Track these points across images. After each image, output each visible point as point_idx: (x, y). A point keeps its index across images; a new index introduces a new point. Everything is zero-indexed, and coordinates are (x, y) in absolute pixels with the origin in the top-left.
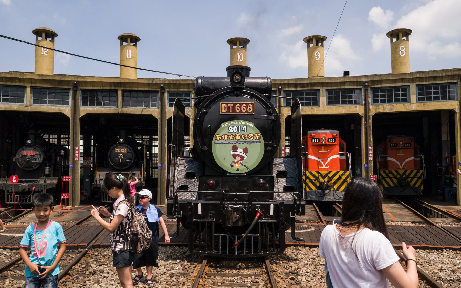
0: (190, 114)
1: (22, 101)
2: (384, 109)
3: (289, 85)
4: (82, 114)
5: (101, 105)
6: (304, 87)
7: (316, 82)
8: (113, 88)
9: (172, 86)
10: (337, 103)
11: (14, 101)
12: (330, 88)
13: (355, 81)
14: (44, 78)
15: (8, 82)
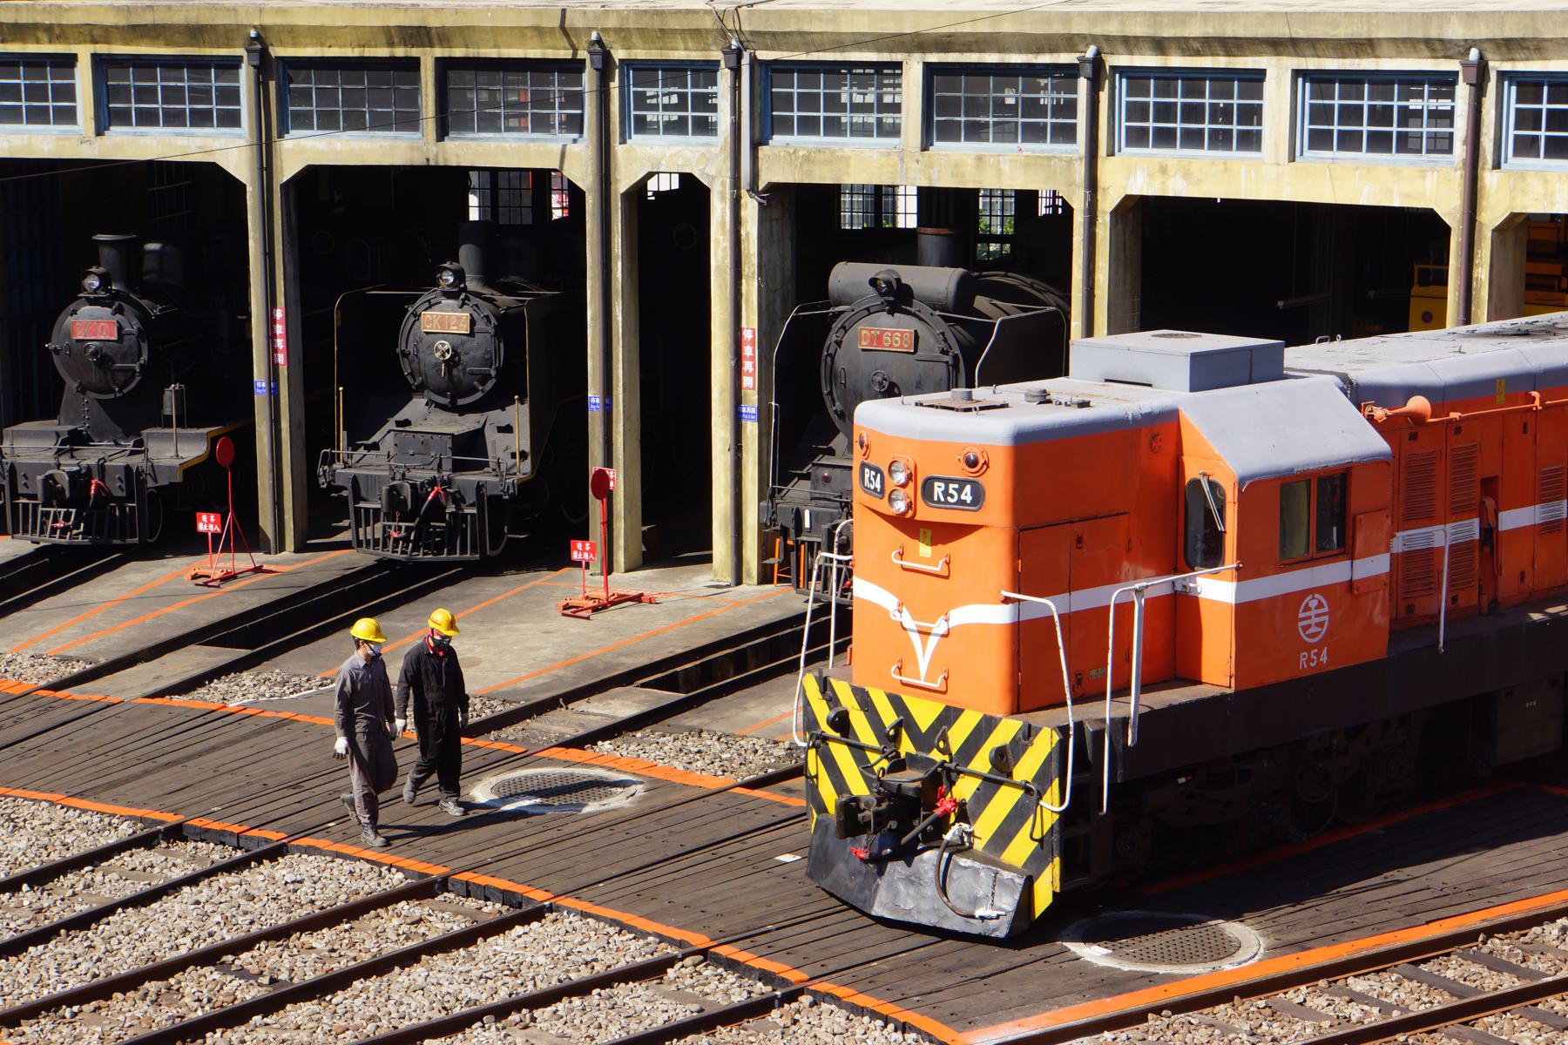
0: (711, 170)
1: (68, 116)
2: (1549, 195)
3: (1129, 43)
4: (288, 168)
5: (364, 128)
6: (1197, 53)
7: (1241, 33)
8: (400, 52)
9: (635, 39)
10: (1349, 142)
11: (37, 116)
12: (1311, 63)
13: (1418, 40)
14: (136, 20)
15: (13, 41)
